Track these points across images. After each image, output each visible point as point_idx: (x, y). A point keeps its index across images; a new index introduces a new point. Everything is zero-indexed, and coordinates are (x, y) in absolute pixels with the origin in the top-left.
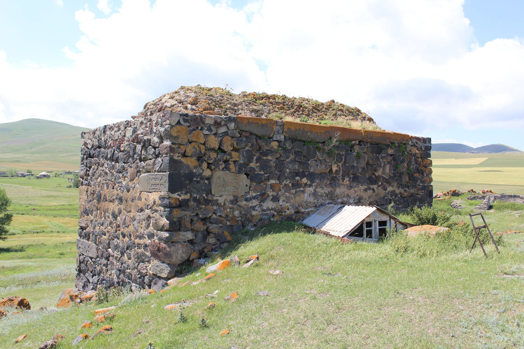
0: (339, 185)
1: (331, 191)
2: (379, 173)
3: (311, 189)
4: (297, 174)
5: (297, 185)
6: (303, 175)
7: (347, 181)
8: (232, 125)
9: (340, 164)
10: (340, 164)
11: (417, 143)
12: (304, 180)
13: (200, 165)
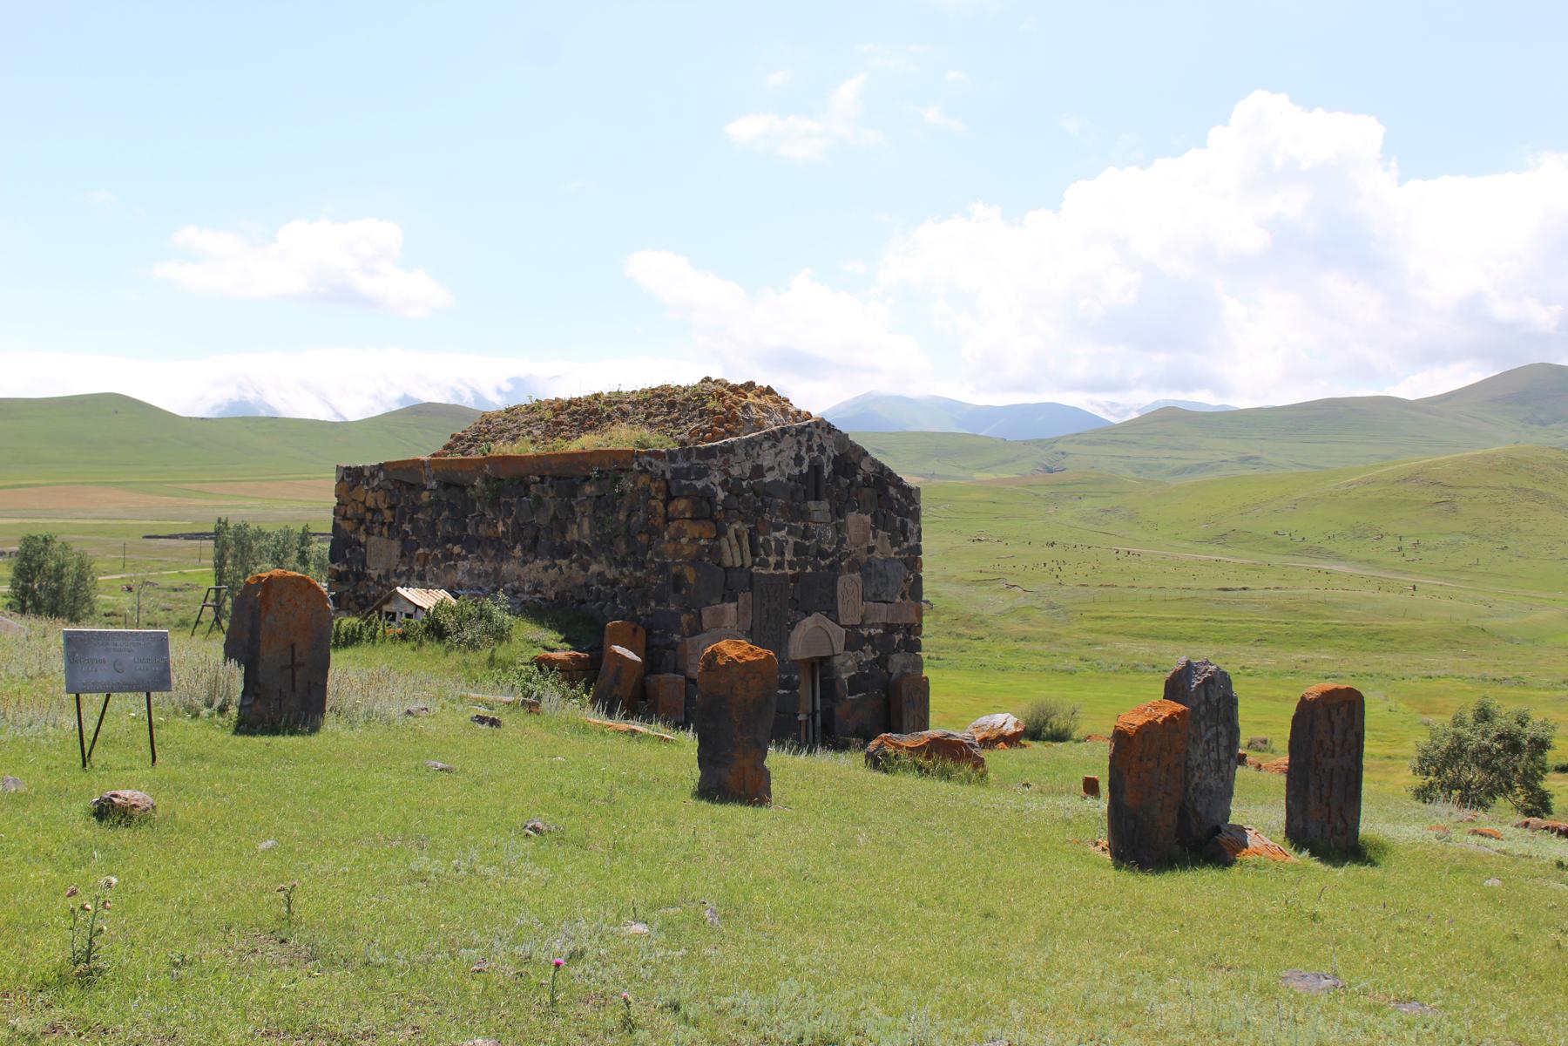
0: (508, 558)
1: (495, 570)
2: (573, 534)
3: (466, 564)
4: (447, 539)
5: (449, 556)
6: (458, 541)
7: (518, 552)
8: (382, 475)
9: (509, 521)
10: (509, 521)
11: (651, 464)
12: (457, 549)
13: (358, 529)
